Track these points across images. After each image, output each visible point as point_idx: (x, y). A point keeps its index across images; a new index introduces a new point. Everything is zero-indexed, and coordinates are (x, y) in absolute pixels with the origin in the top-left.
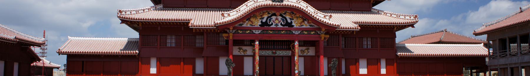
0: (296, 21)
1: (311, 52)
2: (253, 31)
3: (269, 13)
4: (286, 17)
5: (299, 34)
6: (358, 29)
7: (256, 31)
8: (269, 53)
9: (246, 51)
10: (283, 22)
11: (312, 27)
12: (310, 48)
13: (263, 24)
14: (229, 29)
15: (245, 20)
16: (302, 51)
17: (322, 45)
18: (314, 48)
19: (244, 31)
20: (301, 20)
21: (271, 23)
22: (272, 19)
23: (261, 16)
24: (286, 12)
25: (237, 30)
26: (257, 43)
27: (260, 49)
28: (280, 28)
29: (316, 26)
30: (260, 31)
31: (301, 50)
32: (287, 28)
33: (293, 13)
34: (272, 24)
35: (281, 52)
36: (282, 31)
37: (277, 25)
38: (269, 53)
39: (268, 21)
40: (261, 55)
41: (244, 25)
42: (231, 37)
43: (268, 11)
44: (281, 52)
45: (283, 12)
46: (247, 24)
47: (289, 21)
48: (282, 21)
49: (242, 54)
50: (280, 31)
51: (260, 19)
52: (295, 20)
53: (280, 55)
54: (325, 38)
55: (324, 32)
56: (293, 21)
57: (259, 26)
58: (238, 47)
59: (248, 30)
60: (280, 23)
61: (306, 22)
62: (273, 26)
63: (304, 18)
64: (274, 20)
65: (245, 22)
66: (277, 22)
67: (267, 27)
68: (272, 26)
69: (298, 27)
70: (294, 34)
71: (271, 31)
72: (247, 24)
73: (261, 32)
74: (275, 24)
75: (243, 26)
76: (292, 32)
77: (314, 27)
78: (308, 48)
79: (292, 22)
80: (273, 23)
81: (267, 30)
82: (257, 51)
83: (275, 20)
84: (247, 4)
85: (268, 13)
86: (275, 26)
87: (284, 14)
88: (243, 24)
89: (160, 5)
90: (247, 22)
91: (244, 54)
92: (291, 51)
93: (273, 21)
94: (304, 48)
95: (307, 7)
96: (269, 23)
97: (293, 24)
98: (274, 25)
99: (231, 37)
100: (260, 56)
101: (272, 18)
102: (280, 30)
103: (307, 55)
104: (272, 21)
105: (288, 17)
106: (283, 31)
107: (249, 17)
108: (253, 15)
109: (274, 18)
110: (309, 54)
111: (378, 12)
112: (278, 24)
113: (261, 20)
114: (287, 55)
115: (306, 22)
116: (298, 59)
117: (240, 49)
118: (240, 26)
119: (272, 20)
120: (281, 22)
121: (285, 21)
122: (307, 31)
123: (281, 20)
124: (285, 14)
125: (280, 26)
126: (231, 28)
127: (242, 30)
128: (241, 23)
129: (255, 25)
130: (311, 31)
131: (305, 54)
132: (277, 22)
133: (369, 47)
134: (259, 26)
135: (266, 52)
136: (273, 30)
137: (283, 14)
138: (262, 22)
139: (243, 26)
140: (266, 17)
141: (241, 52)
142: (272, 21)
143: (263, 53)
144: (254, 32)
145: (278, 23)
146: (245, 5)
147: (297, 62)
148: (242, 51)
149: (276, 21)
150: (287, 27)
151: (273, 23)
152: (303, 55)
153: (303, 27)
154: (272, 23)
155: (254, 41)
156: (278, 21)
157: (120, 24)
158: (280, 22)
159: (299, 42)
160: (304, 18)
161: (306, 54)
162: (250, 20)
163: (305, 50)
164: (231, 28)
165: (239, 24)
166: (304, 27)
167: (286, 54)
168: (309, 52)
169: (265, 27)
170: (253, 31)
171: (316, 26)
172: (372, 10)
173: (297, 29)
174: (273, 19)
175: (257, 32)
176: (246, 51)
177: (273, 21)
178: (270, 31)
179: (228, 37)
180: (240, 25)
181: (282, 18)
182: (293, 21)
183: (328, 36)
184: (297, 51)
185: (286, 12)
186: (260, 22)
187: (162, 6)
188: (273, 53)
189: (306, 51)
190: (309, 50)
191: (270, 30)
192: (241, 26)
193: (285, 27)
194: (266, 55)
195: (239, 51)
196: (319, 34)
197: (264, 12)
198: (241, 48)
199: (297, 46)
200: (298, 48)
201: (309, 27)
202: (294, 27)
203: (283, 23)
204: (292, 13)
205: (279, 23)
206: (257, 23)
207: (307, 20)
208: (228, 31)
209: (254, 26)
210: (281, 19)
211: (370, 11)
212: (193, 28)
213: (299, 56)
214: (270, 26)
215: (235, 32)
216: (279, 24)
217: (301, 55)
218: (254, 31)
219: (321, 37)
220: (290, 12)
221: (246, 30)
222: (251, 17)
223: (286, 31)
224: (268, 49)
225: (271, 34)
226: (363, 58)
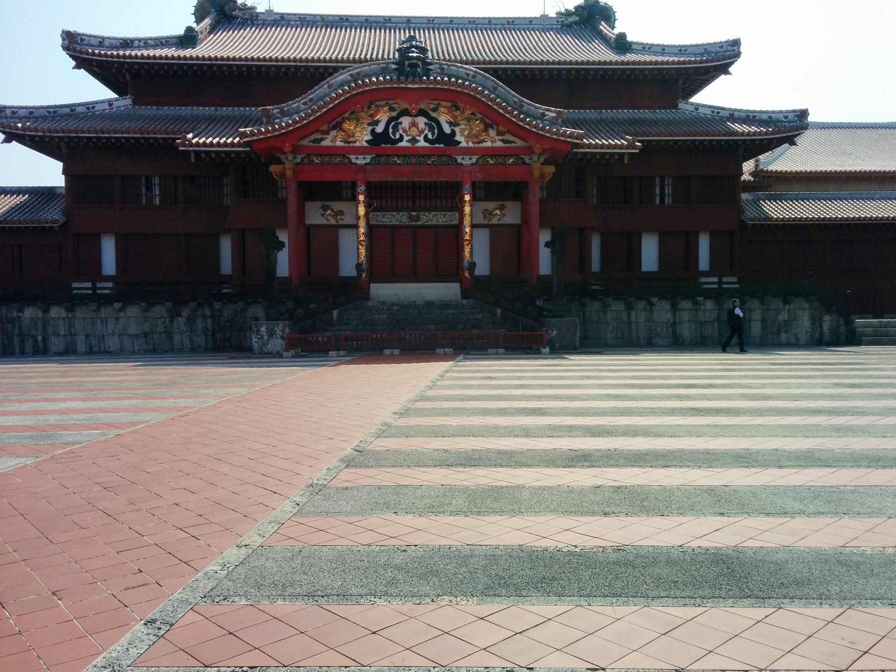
0: (464, 130)
1: (511, 215)
2: (351, 156)
3: (393, 107)
4: (439, 119)
5: (472, 164)
6: (635, 147)
7: (358, 156)
8: (400, 218)
9: (341, 213)
10: (429, 131)
11: (508, 145)
12: (508, 204)
13: (378, 139)
14: (281, 151)
15: (325, 128)
16: (488, 213)
17: (536, 194)
18: (520, 203)
19: (327, 159)
20: (478, 126)
21: (398, 136)
22: (401, 123)
23: (372, 116)
24: (439, 104)
25: (309, 155)
26: (362, 188)
27: (368, 206)
28: (423, 148)
29: (519, 143)
30: (368, 159)
31: (484, 210)
32: (442, 147)
33: (458, 109)
34: (401, 139)
35: (431, 215)
36: (429, 156)
37: (413, 140)
38: (400, 218)
39: (391, 130)
40: (381, 223)
41: (327, 143)
42: (289, 173)
43: (391, 102)
44: (431, 215)
45: (432, 106)
46: (333, 140)
47: (447, 129)
48: (427, 127)
49: (333, 221)
50: (423, 156)
51: (369, 124)
52: (463, 127)
53: (430, 223)
54: (542, 175)
55: (542, 160)
56: (457, 129)
57: (365, 144)
58: (319, 204)
59: (338, 155)
60: (423, 136)
61: (492, 133)
62: (404, 144)
63: (487, 120)
64: (407, 128)
65: (327, 133)
66: (414, 131)
67: (389, 145)
68: (400, 144)
69: (471, 144)
70: (461, 164)
71: (398, 156)
72: (333, 140)
73: (371, 160)
74: (410, 137)
75: (324, 143)
76: (456, 160)
77: (513, 145)
78: (503, 205)
79: (453, 133)
80: (404, 135)
81: (388, 156)
82: (362, 210)
83: (410, 128)
84: (330, 83)
85: (389, 109)
86: (409, 145)
87: (434, 112)
88: (322, 139)
89: (124, 97)
90: (333, 133)
91: (337, 220)
92: (457, 214)
93: (405, 131)
94: (490, 205)
95: (495, 89)
96: (394, 134)
97: (458, 138)
98: (407, 141)
99: (289, 173)
100: (370, 228)
101: (400, 121)
102: (422, 154)
103: (498, 223)
104: (401, 132)
105: (444, 119)
106: (431, 155)
107: (339, 119)
108: (351, 114)
109: (406, 121)
110: (505, 221)
111: (697, 109)
112: (418, 138)
113: (370, 128)
114: (447, 223)
115: (492, 133)
116: (471, 231)
117: (325, 208)
118: (316, 144)
119: (400, 127)
120: (426, 132)
121: (436, 131)
122: (495, 156)
123: (424, 126)
124: (435, 110)
125: (422, 143)
126: (287, 147)
127: (321, 156)
128: (318, 136)
129: (355, 142)
130: (505, 156)
131: (495, 221)
132: (414, 131)
133: (668, 200)
134: (365, 144)
135: (393, 215)
136: (406, 153)
137: (430, 110)
138: (373, 132)
139: (324, 143)
140: (383, 117)
141: (328, 217)
142: (401, 132)
143: (384, 220)
144: (354, 161)
145: (418, 135)
146: (326, 86)
147: (467, 240)
148: (330, 214)
149: (412, 129)
150: (442, 145)
151: (404, 135)
152: (490, 223)
153: (484, 145)
154: (401, 135)
155: (354, 185)
156: (418, 129)
157: (2, 143)
158: (422, 132)
159: (473, 184)
160: (487, 120)
161: (498, 220)
162: (341, 129)
163: (496, 209)
164: (287, 147)
165: (312, 138)
166: (488, 144)
167: (445, 222)
168: (504, 215)
169: (383, 145)
170: (351, 156)
171: (519, 143)
172: (680, 106)
173: (468, 151)
174: (403, 125)
175: (361, 160)
176: (341, 213)
177: (405, 131)
178: (395, 159)
179: (283, 175)
180: (315, 141)
181: (426, 121)
182: (457, 129)
183: (551, 169)
184: (467, 209)
185: (439, 104)
186: (369, 132)
187: (131, 99)
188: (411, 218)
189: (498, 212)
190: (505, 209)
191: (396, 155)
192: (319, 143)
193: (437, 145)
194: (395, 222)
195: (323, 215)
196: (529, 164)
197: (378, 106)
198: (329, 206)
199: (467, 198)
200: (470, 201)
201: (499, 144)
202: (461, 145)
203: (430, 136)
204: (454, 108)
205: (420, 136)
206: (363, 137)
207: (495, 127)
208: (282, 157)
209: (351, 145)
210: (426, 124)
211: (675, 107)
212: (189, 151)
213: (473, 226)
214: (397, 143)
215: (302, 160)
216: (421, 138)
217: (486, 222)
218: (353, 158)
219: (532, 173)
220: (449, 104)
221: (331, 155)
222: (343, 120)
223: (439, 156)
224: (398, 209)
225: (400, 164)
226: (651, 230)
